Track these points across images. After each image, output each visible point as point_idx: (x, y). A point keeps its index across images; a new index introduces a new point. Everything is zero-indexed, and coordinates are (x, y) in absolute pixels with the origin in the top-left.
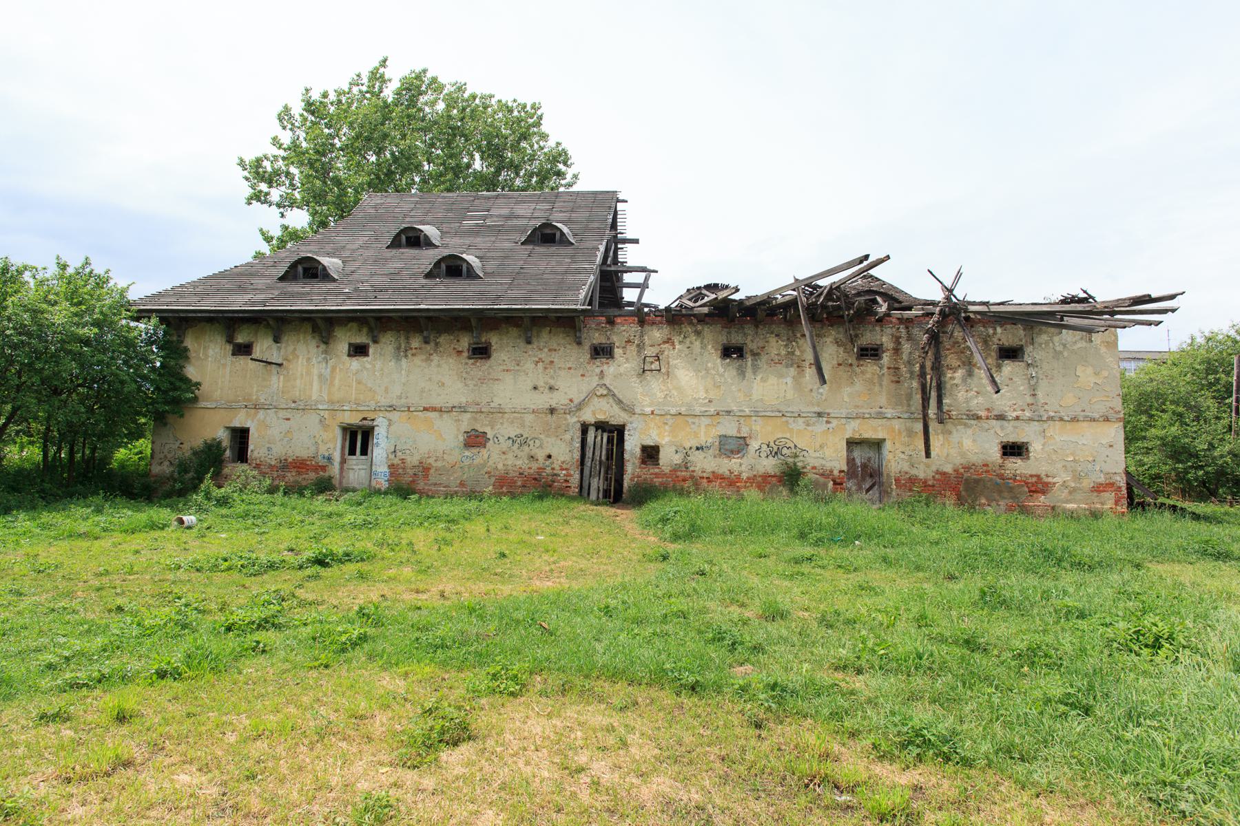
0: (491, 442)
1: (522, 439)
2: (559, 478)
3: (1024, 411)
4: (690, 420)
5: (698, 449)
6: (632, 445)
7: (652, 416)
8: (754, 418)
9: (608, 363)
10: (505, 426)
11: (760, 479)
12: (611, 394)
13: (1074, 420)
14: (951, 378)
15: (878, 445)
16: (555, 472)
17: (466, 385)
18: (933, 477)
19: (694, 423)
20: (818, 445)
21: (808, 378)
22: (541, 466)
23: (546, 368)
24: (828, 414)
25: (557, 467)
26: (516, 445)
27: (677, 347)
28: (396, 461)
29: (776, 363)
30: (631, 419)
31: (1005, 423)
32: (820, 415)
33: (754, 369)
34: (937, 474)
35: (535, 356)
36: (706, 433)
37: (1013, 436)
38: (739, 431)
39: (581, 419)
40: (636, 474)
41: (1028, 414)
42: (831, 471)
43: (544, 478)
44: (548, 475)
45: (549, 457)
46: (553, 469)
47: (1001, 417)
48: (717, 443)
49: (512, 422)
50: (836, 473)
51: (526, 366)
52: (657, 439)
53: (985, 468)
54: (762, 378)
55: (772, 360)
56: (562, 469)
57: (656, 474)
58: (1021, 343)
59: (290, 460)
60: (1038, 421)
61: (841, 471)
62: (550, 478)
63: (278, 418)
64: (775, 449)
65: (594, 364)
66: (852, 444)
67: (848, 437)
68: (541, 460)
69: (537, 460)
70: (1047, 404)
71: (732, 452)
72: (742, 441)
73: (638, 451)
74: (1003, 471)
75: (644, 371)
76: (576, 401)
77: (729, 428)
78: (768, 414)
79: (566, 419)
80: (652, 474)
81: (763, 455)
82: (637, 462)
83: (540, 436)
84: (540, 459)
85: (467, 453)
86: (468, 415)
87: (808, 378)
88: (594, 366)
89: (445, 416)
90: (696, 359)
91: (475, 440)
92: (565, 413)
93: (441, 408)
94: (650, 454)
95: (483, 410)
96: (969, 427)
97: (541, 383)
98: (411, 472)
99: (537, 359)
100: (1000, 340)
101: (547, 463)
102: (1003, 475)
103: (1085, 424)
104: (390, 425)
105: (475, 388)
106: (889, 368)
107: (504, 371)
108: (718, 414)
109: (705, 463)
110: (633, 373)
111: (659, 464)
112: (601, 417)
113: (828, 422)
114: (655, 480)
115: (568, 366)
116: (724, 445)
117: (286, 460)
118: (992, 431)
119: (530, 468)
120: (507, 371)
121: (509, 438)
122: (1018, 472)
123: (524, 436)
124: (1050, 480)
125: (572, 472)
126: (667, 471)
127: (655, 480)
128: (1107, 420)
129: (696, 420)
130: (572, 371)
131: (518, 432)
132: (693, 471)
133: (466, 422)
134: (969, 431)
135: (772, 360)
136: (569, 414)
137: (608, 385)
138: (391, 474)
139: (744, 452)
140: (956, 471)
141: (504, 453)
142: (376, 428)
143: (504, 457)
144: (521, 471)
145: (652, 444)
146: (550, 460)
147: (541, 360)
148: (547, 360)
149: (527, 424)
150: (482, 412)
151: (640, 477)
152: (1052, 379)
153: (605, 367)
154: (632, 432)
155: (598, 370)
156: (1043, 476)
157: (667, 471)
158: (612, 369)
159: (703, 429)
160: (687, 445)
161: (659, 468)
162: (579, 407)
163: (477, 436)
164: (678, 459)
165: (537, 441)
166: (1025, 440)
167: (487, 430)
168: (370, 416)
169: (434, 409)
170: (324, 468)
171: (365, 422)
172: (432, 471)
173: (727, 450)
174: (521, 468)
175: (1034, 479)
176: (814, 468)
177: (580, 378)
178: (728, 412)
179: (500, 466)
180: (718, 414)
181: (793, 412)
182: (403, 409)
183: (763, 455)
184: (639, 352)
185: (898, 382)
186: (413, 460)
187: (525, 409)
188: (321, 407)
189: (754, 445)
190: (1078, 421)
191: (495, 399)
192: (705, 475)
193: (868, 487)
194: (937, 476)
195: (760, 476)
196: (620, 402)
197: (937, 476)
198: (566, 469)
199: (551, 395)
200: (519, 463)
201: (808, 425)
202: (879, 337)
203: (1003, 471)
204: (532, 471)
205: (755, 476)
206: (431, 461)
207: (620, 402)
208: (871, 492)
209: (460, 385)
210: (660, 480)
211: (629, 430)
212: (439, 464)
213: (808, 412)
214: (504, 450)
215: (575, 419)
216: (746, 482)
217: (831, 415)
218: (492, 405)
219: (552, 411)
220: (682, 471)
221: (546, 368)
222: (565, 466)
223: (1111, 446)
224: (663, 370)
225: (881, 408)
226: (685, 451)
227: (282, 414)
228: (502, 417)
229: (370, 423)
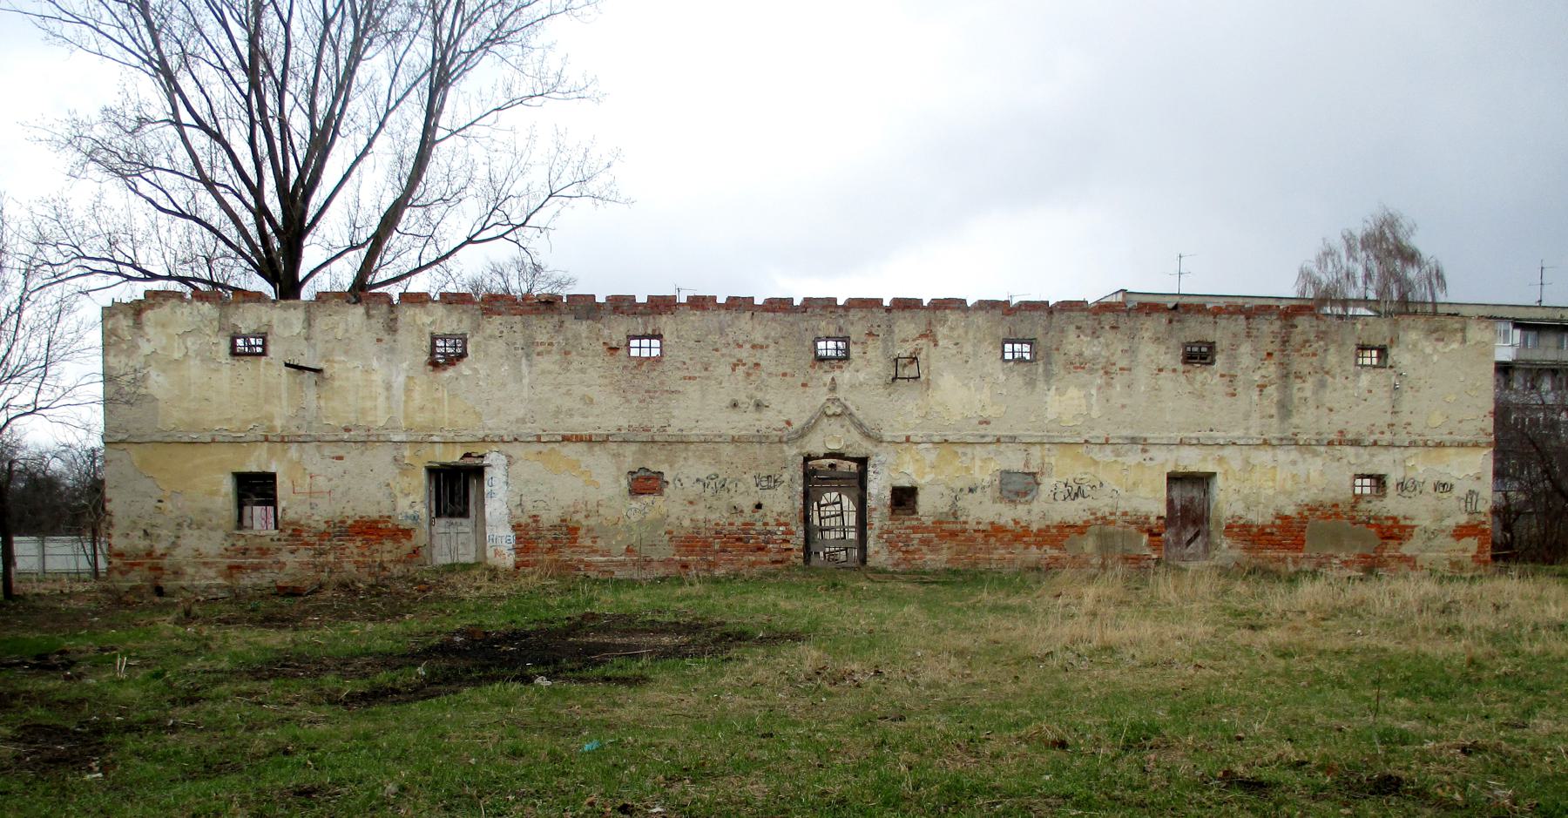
0: (671, 486)
1: (718, 481)
2: (775, 537)
3: (1382, 433)
4: (960, 449)
6: (879, 487)
7: (907, 445)
8: (1047, 446)
9: (841, 367)
10: (690, 463)
11: (1054, 531)
12: (845, 413)
13: (1440, 445)
14: (1299, 389)
15: (1202, 480)
16: (768, 528)
17: (628, 401)
18: (1273, 523)
19: (965, 454)
20: (1130, 482)
21: (1118, 389)
22: (748, 520)
23: (748, 375)
24: (1145, 439)
25: (771, 521)
26: (709, 491)
27: (940, 343)
28: (524, 520)
29: (1076, 368)
30: (876, 450)
31: (1361, 450)
32: (1134, 441)
33: (1047, 376)
34: (1277, 518)
35: (730, 355)
36: (984, 468)
37: (1370, 466)
38: (1026, 465)
39: (804, 451)
40: (886, 528)
41: (1387, 437)
42: (1147, 518)
43: (752, 538)
44: (759, 534)
45: (759, 506)
46: (766, 524)
47: (1356, 443)
48: (997, 482)
49: (702, 457)
50: (1153, 519)
51: (719, 371)
52: (917, 479)
53: (1334, 509)
54: (1057, 389)
55: (1071, 363)
56: (779, 524)
57: (913, 528)
58: (1384, 343)
59: (350, 522)
61: (1159, 518)
62: (762, 537)
63: (323, 457)
64: (1075, 488)
65: (821, 368)
66: (1174, 479)
67: (1169, 471)
68: (748, 510)
69: (742, 511)
70: (1409, 424)
71: (1017, 494)
72: (1030, 479)
73: (888, 494)
74: (1355, 514)
75: (894, 379)
76: (797, 425)
77: (1013, 460)
78: (1066, 440)
79: (782, 451)
80: (908, 528)
81: (1060, 497)
82: (887, 511)
83: (745, 476)
84: (746, 510)
85: (635, 504)
86: (634, 447)
87: (1118, 389)
88: (821, 371)
89: (597, 448)
90: (967, 362)
91: (645, 484)
92: (780, 442)
93: (590, 436)
94: (904, 498)
95: (656, 438)
96: (1318, 455)
97: (742, 397)
98: (550, 535)
99: (734, 361)
100: (1360, 338)
101: (757, 515)
102: (1354, 517)
103: (1452, 451)
104: (509, 464)
105: (642, 405)
106: (1222, 376)
107: (685, 378)
108: (998, 441)
109: (984, 510)
110: (877, 381)
111: (915, 512)
112: (834, 446)
113: (1144, 451)
114: (912, 536)
115: (781, 370)
116: (1007, 484)
117: (343, 522)
118: (1345, 461)
119: (731, 524)
120: (690, 378)
121: (698, 480)
122: (1372, 514)
123: (721, 477)
124: (1408, 522)
125: (794, 529)
126: (929, 523)
127: (912, 536)
128: (1476, 445)
129: (969, 450)
130: (788, 378)
131: (711, 471)
132: (965, 523)
133: (631, 458)
134: (1319, 461)
135: (1071, 363)
136: (787, 443)
137: (842, 400)
138: (518, 538)
139: (1034, 493)
141: (691, 503)
142: (487, 469)
143: (691, 508)
144: (719, 528)
145: (907, 485)
146: (761, 511)
148: (750, 361)
149: (724, 458)
150: (653, 442)
151: (892, 532)
152: (1418, 391)
153: (837, 373)
154: (879, 468)
155: (827, 378)
156: (1400, 517)
157: (929, 523)
158: (847, 375)
159: (978, 463)
160: (959, 484)
161: (917, 519)
162: (803, 433)
163: (648, 479)
164: (943, 506)
165: (740, 485)
167: (664, 468)
168: (478, 450)
169: (579, 439)
170: (407, 533)
171: (468, 461)
172: (582, 532)
173: (1010, 492)
174: (717, 524)
175: (1390, 523)
176: (1125, 514)
177: (801, 389)
178: (1013, 439)
179: (686, 523)
180: (998, 441)
181: (1098, 437)
182: (529, 439)
183: (1060, 497)
184: (886, 349)
185: (1234, 395)
186: (550, 517)
187: (720, 436)
189: (1047, 484)
190: (1444, 446)
191: (672, 421)
192: (981, 527)
193: (1189, 537)
194: (1278, 522)
195: (1055, 527)
196: (860, 426)
197: (1278, 522)
198: (786, 524)
199: (757, 416)
200: (714, 517)
201: (1118, 455)
202: (1211, 332)
203: (1355, 514)
204: (735, 528)
205: (1048, 526)
206: (579, 517)
207: (860, 426)
208: (1192, 545)
209: (616, 400)
210: (920, 536)
211: (875, 466)
212: (592, 522)
213: (1119, 438)
214: (691, 498)
215: (794, 451)
216: (1036, 535)
217: (1149, 441)
218: (670, 431)
219: (761, 439)
220: (949, 523)
221: (748, 375)
222: (782, 519)
223: (1478, 478)
224: (923, 377)
225: (1211, 430)
226: (954, 494)
227: (328, 450)
228: (686, 449)
229: (477, 461)
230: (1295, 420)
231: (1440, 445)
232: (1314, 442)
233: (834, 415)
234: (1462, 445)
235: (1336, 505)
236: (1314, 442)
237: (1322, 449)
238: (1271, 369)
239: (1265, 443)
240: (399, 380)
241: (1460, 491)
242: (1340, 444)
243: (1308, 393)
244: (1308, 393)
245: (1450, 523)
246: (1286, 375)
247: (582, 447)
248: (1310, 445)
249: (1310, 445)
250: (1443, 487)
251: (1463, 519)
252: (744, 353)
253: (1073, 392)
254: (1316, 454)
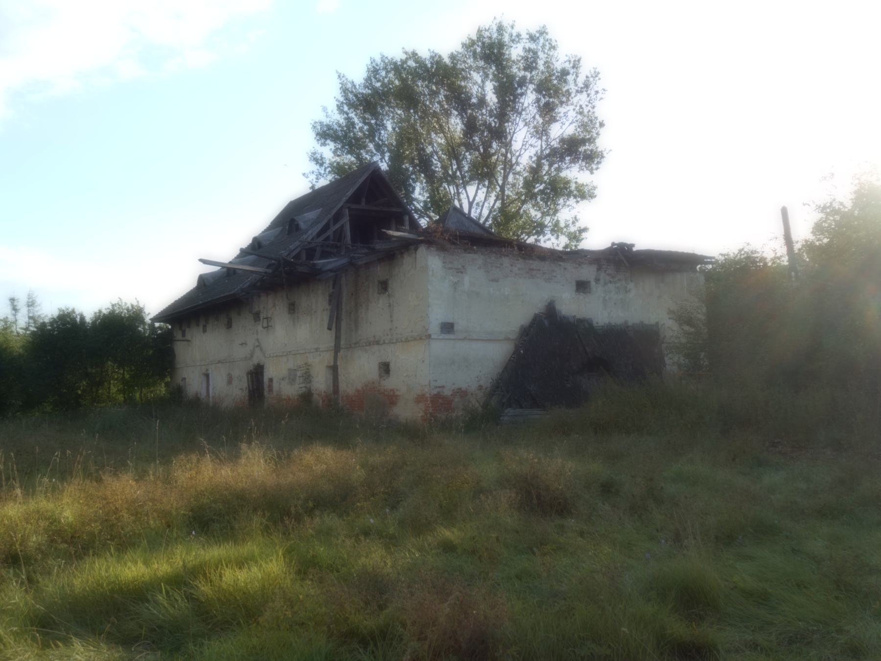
5: (283, 379)
8: (298, 355)
13: (407, 341)
60: (393, 343)
61: (325, 392)
128: (421, 339)
140: (362, 388)
162: (252, 356)
166: (388, 361)
178: (290, 352)
188: (198, 364)
190: (409, 341)
223: (423, 361)
232: (364, 344)
233: (257, 346)
234: (415, 339)
235: (373, 383)
236: (364, 344)
237: (367, 348)
242: (373, 344)
248: (363, 346)
249: (363, 346)
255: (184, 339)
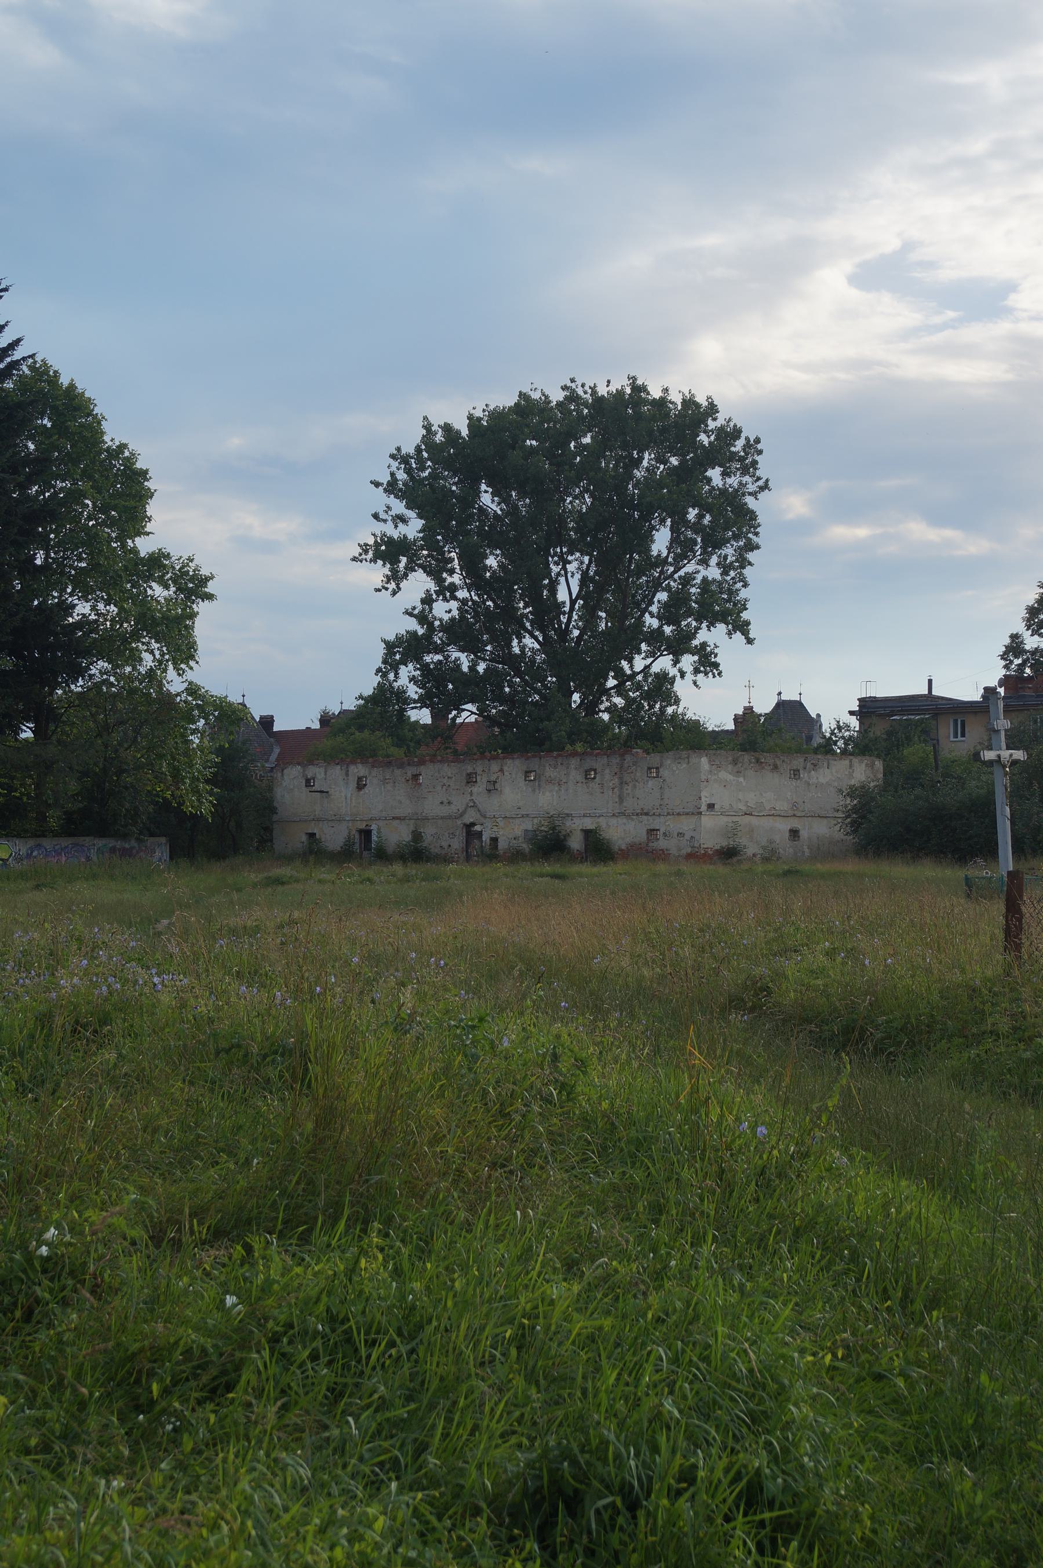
13: (679, 814)
47: (647, 814)
147: (444, 785)
162: (462, 815)
215: (459, 822)
219: (450, 817)
230: (625, 804)
231: (679, 814)
234: (687, 814)
238: (616, 781)
239: (614, 815)
240: (349, 795)
241: (688, 837)
243: (629, 791)
244: (629, 791)
245: (684, 852)
246: (622, 783)
247: (398, 821)
250: (681, 834)
251: (689, 850)
252: (445, 781)
253: (548, 794)
254: (633, 820)
255: (317, 788)
